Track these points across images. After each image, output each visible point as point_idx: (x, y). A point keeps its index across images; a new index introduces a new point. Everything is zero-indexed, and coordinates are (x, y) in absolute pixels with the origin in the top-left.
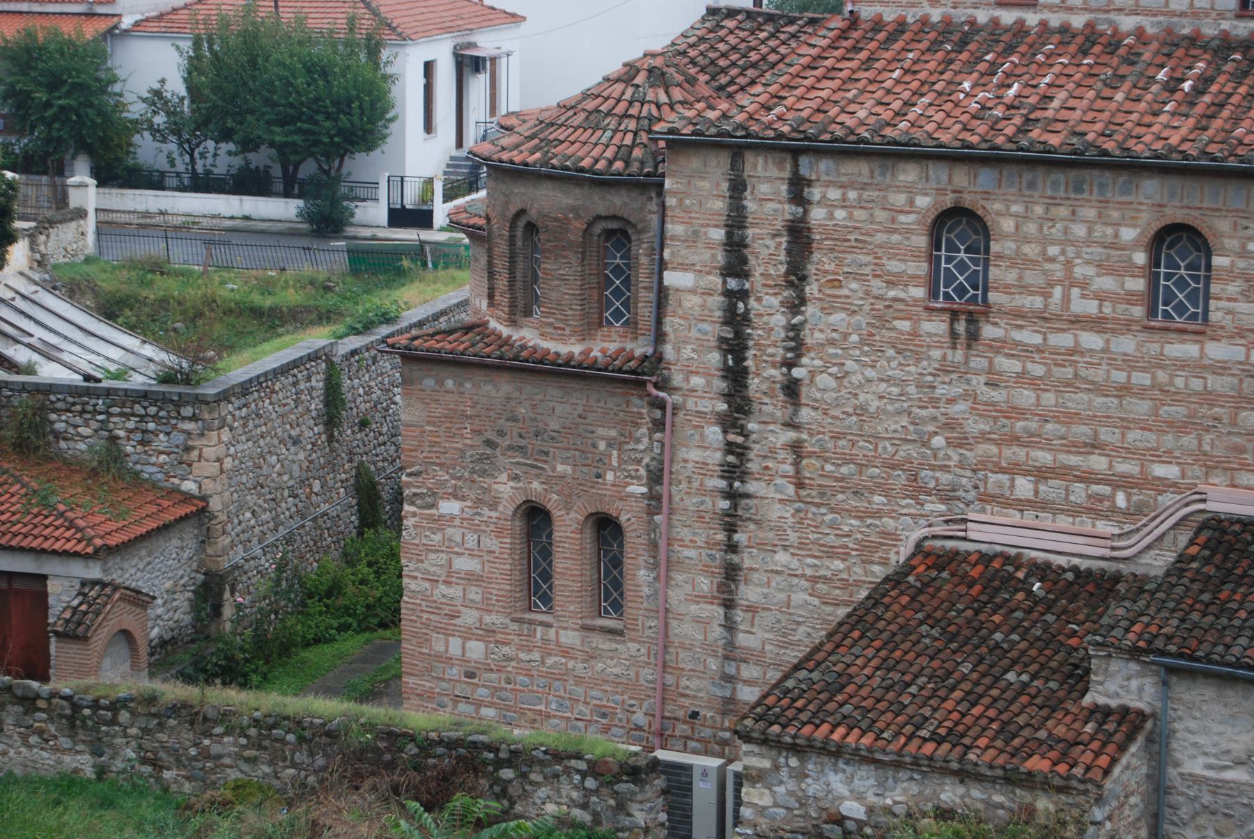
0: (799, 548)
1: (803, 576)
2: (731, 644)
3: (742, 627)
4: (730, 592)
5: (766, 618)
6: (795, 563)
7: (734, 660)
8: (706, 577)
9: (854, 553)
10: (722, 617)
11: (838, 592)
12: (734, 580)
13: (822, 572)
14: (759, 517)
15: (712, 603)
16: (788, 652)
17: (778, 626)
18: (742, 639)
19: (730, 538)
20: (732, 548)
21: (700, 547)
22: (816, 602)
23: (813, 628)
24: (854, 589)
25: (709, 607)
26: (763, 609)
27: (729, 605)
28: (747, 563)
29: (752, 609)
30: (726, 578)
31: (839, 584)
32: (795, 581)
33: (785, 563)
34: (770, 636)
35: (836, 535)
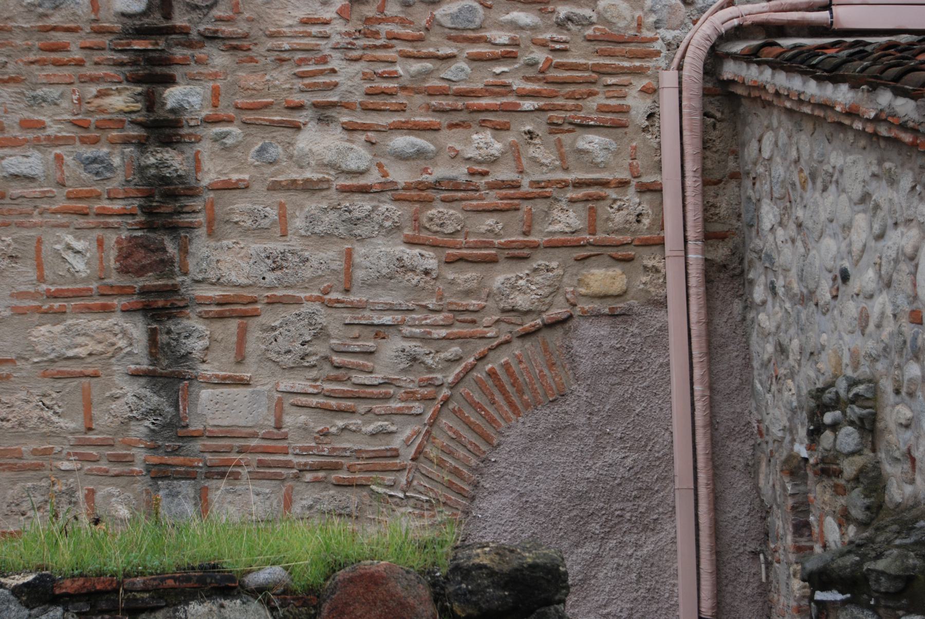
0: (366, 109)
1: (386, 188)
2: (172, 431)
3: (208, 370)
4: (164, 266)
5: (281, 329)
6: (358, 156)
7: (189, 475)
8: (79, 231)
9: (528, 104)
10: (140, 347)
11: (490, 221)
12: (173, 229)
13: (439, 172)
14: (241, 28)
15: (106, 310)
16: (354, 422)
17: (321, 349)
18: (211, 407)
19: (151, 102)
20: (163, 129)
21: (56, 141)
22: (430, 260)
23: (425, 339)
24: (540, 206)
25: (97, 323)
26: (273, 302)
27: (160, 308)
28: (211, 173)
29: (235, 309)
30: (149, 227)
31: (492, 199)
32: (363, 205)
33: (329, 157)
34: (300, 384)
35: (474, 59)
